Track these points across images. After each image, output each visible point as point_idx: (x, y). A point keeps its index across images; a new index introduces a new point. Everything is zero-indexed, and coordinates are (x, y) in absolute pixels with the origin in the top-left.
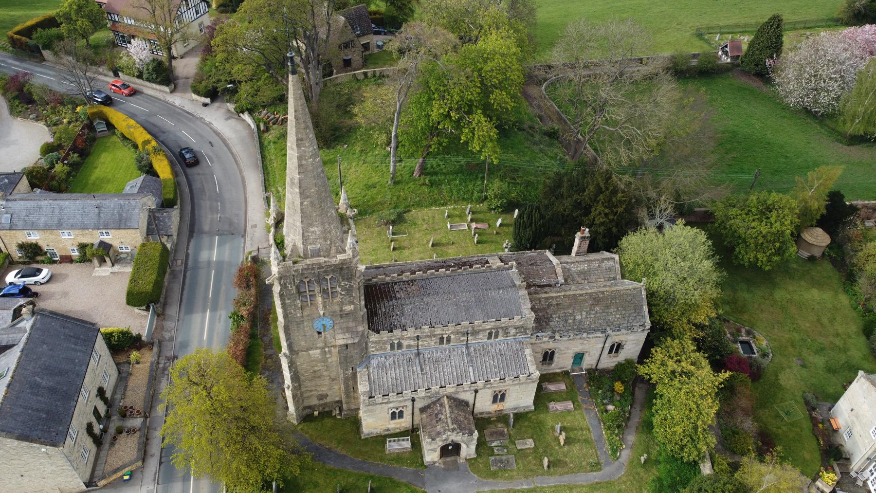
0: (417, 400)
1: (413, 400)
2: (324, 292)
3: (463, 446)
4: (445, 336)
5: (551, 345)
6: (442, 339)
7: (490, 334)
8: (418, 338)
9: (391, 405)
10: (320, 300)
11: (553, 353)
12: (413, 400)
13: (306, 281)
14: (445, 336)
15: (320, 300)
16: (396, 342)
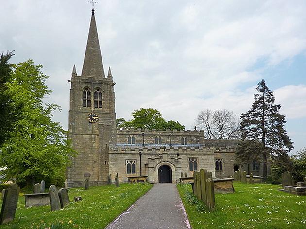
0: (143, 155)
1: (141, 154)
2: (96, 102)
3: (173, 169)
4: (158, 137)
5: (219, 155)
6: (156, 138)
7: (183, 139)
8: (143, 135)
9: (127, 157)
10: (92, 101)
11: (221, 162)
12: (141, 154)
13: (87, 91)
14: (158, 137)
15: (92, 101)
16: (131, 136)
